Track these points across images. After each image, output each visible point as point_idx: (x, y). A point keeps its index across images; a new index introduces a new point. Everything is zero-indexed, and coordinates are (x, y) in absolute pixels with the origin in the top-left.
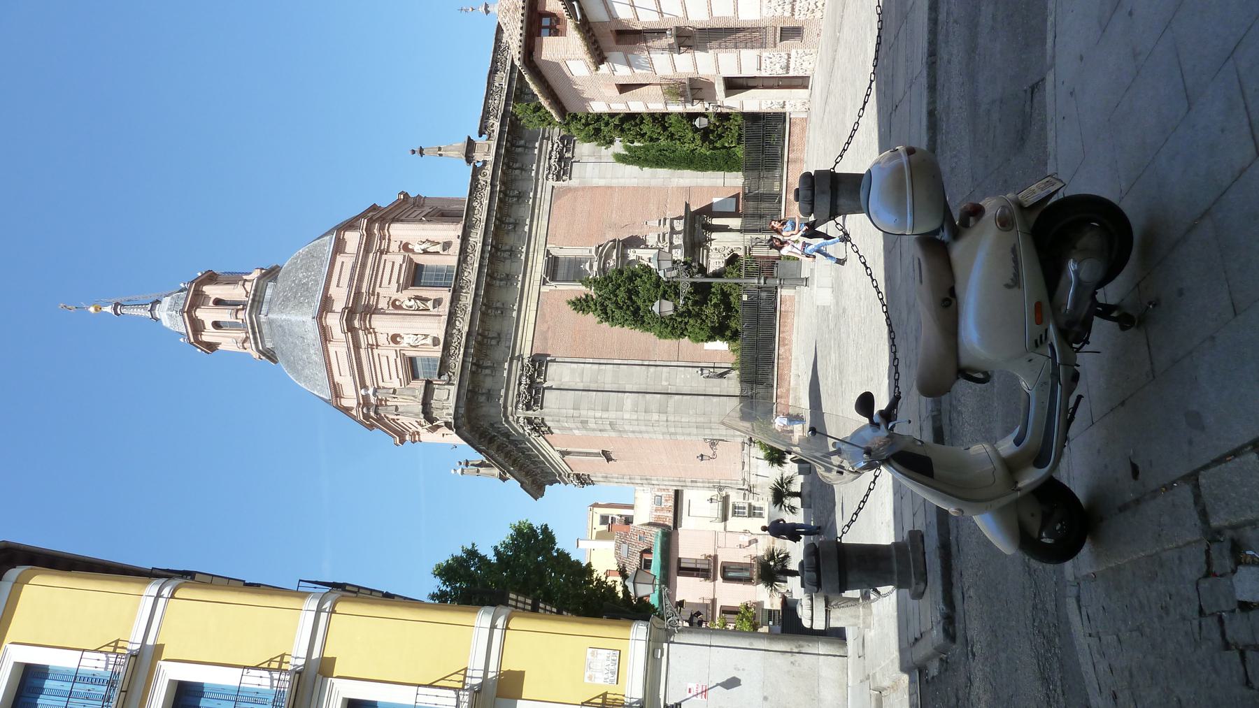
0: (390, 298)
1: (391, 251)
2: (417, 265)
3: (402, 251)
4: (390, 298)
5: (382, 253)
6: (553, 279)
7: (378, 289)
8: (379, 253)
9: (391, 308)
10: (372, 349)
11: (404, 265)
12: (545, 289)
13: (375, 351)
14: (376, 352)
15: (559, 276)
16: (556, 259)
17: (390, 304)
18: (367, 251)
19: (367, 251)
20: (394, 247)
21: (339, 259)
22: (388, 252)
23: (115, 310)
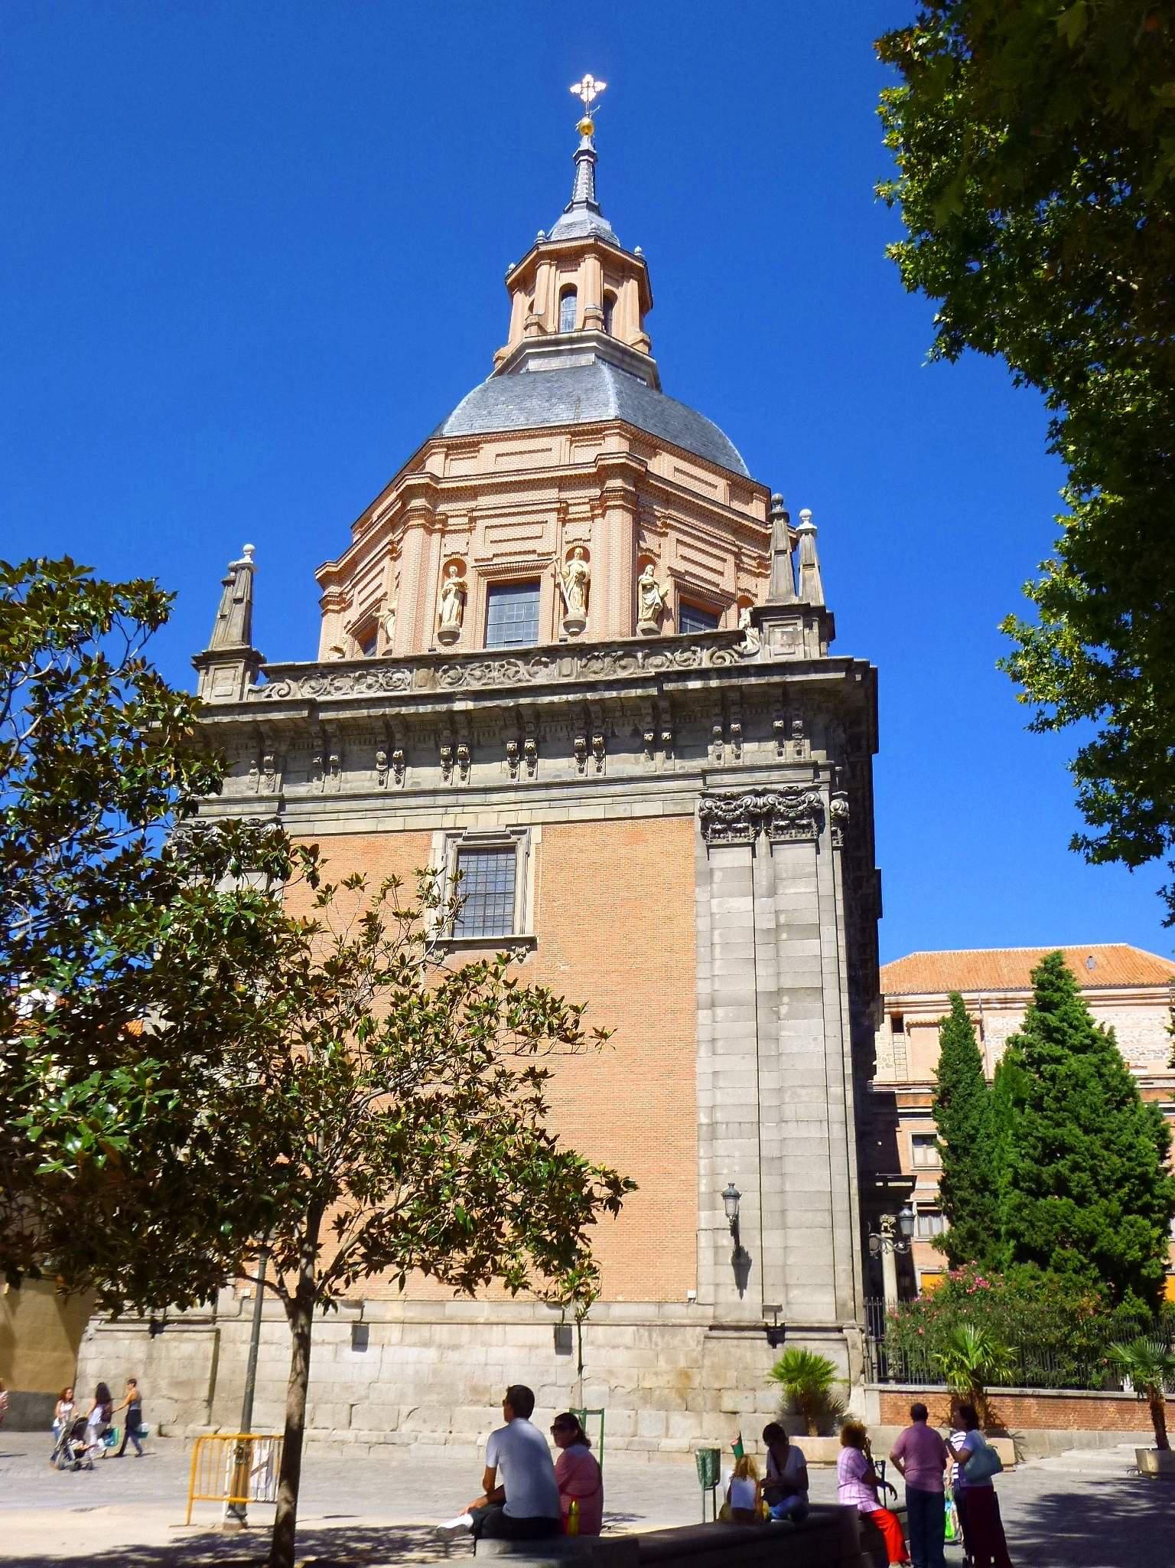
0: (466, 554)
1: (565, 529)
2: (534, 585)
3: (567, 548)
4: (466, 554)
5: (558, 510)
6: (461, 851)
7: (481, 524)
8: (557, 505)
9: (444, 560)
10: (390, 552)
11: (534, 557)
12: (438, 838)
13: (388, 558)
14: (386, 562)
15: (470, 863)
16: (511, 849)
17: (454, 556)
18: (563, 483)
19: (563, 483)
20: (575, 530)
21: (559, 443)
22: (564, 522)
23: (587, 152)
